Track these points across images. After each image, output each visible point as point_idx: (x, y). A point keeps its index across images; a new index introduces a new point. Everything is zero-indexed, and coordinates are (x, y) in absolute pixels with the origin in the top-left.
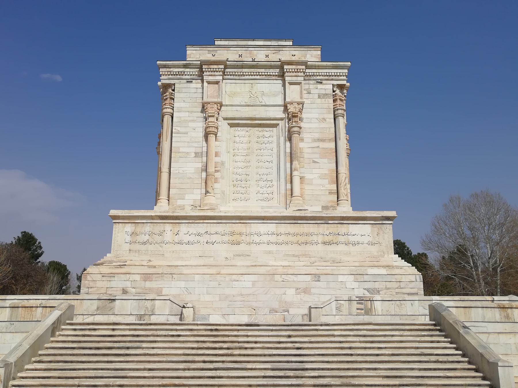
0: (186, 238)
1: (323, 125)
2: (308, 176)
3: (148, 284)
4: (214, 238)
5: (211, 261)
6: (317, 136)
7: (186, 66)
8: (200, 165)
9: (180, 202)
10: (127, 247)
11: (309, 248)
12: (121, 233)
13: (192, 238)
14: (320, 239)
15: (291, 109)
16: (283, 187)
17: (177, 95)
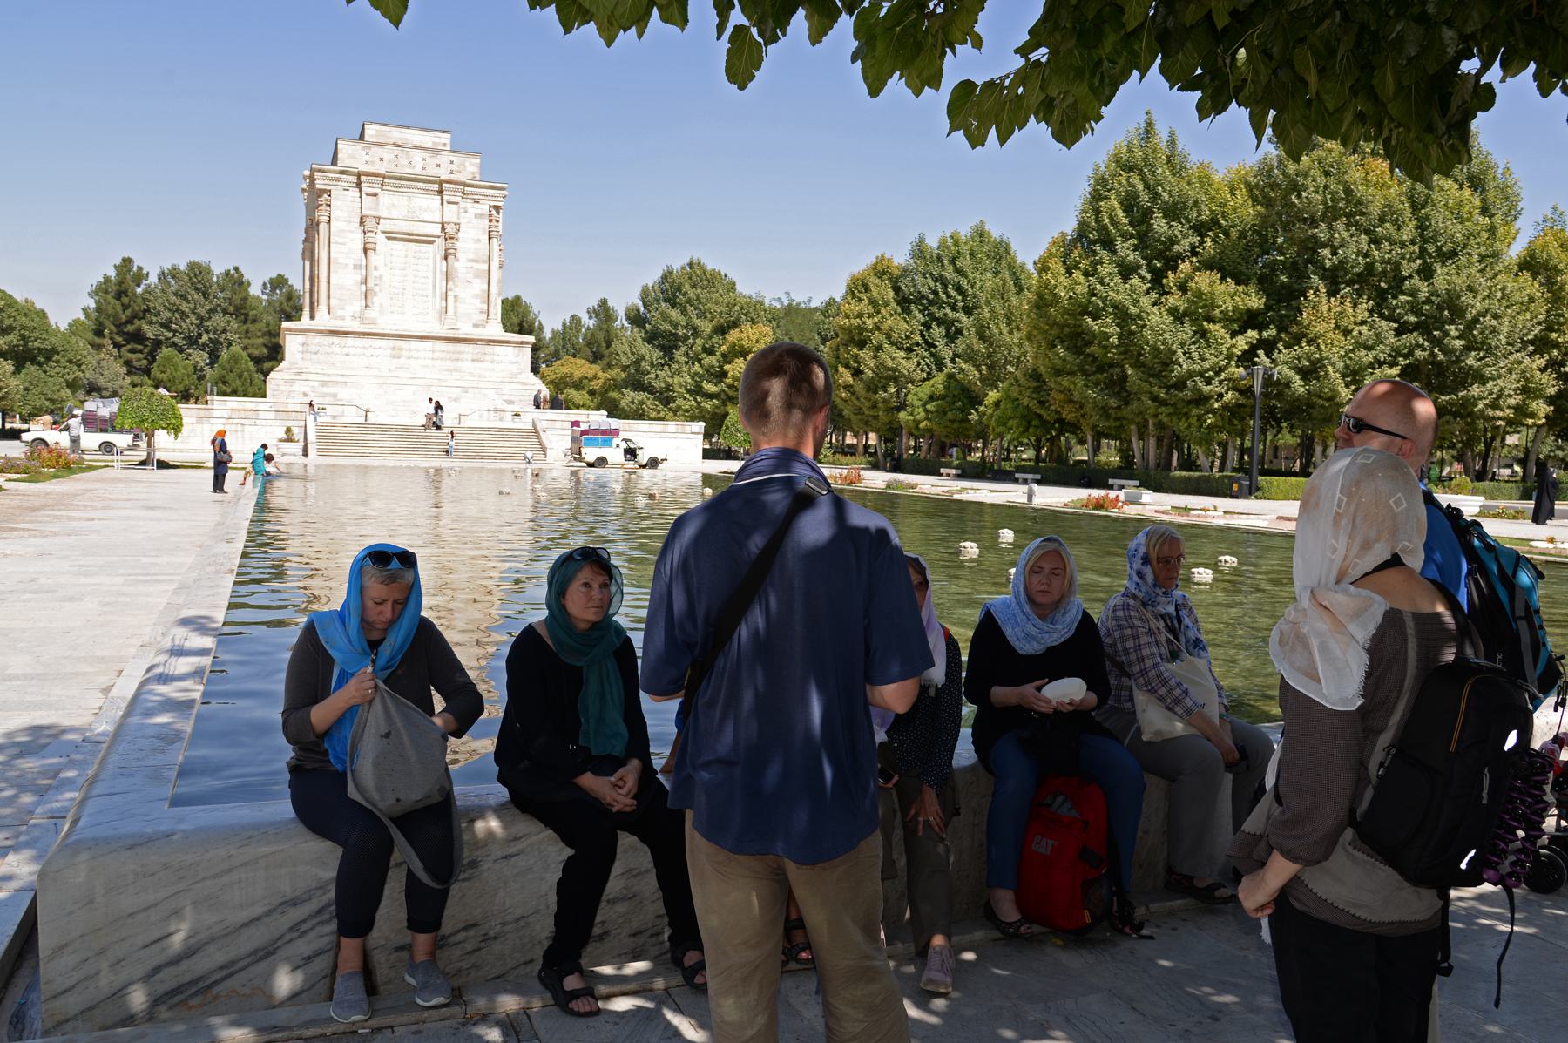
0: (352, 351)
1: (478, 246)
2: (462, 295)
3: (325, 390)
4: (377, 352)
5: (375, 372)
6: (472, 256)
7: (342, 172)
8: (359, 278)
9: (340, 313)
10: (299, 356)
11: (460, 364)
12: (292, 345)
13: (358, 351)
14: (470, 357)
15: (449, 229)
16: (439, 304)
17: (333, 203)
